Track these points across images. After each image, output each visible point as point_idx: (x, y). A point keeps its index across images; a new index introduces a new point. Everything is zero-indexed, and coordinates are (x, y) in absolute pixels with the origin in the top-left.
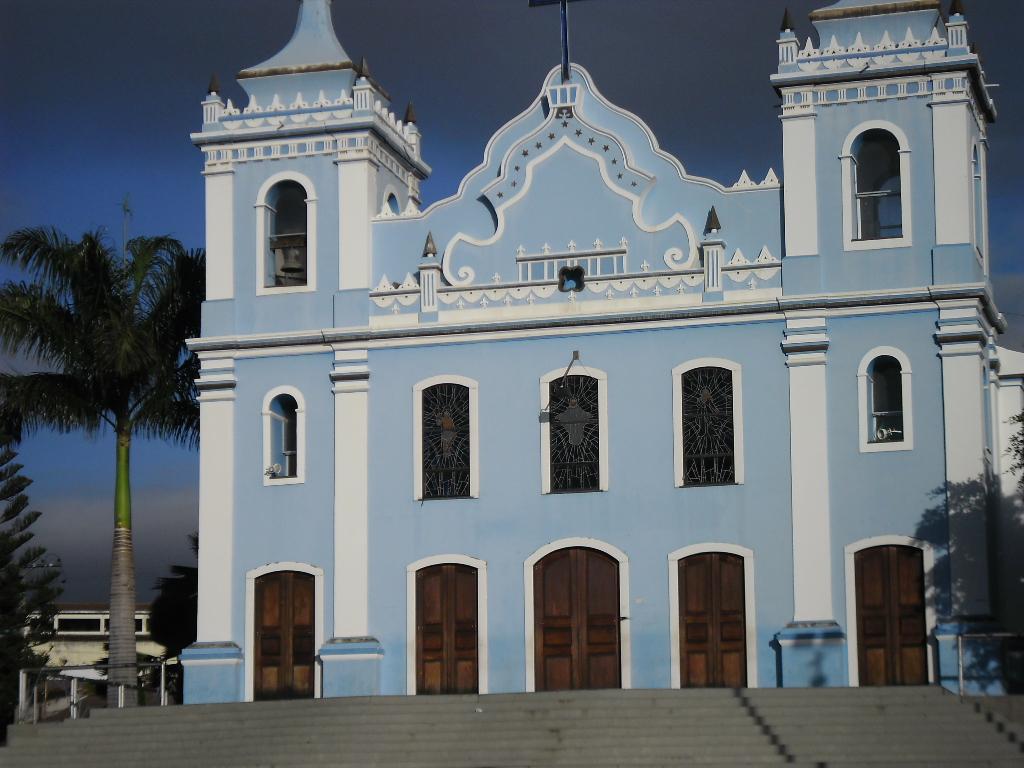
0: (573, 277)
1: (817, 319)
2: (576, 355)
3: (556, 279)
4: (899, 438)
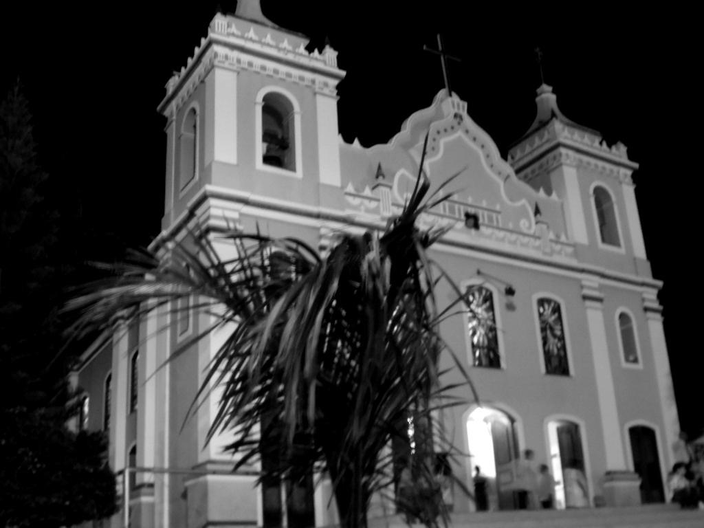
0: (473, 221)
1: (594, 281)
2: (479, 273)
3: (463, 217)
4: (636, 361)
